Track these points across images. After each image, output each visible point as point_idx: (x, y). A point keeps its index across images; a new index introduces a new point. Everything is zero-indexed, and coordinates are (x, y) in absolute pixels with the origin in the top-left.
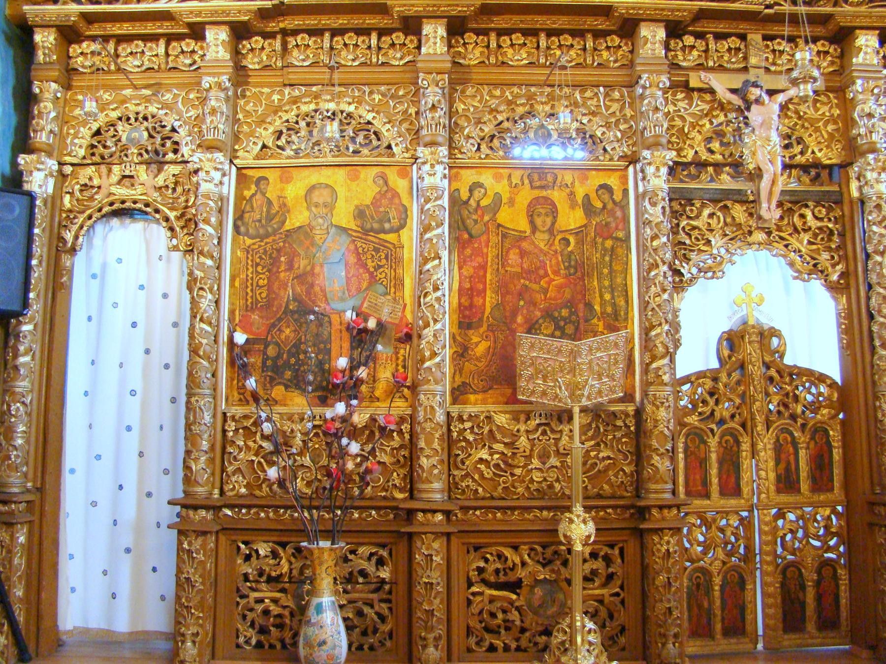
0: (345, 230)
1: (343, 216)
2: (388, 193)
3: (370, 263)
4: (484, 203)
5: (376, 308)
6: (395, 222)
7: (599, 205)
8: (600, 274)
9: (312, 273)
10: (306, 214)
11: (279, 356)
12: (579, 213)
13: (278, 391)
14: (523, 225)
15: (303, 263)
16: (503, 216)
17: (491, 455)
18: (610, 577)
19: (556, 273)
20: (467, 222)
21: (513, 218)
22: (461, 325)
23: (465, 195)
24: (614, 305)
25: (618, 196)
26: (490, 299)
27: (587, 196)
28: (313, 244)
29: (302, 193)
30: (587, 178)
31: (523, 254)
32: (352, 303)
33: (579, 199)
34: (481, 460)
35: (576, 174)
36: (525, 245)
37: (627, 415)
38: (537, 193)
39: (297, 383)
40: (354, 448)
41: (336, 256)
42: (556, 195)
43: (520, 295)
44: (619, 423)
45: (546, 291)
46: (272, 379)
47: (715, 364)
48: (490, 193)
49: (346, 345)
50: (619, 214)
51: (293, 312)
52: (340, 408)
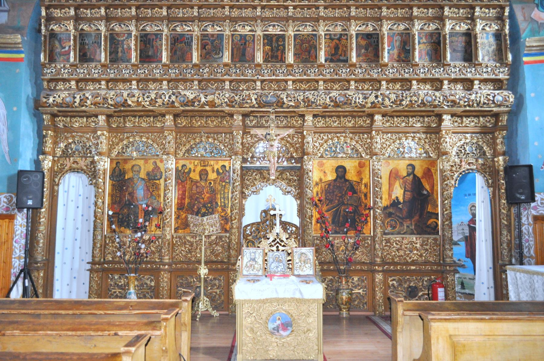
0: (143, 179)
1: (143, 175)
2: (157, 168)
3: (151, 190)
4: (186, 171)
5: (152, 203)
6: (159, 177)
7: (221, 171)
8: (221, 193)
9: (133, 192)
10: (131, 174)
11: (123, 218)
12: (215, 174)
13: (122, 229)
14: (198, 178)
15: (130, 189)
16: (192, 175)
17: (185, 248)
18: (220, 285)
19: (207, 193)
20: (182, 176)
21: (195, 176)
22: (178, 209)
23: (180, 168)
24: (224, 203)
25: (227, 169)
26: (187, 201)
27: (218, 169)
28: (134, 183)
29: (130, 167)
30: (218, 163)
31: (197, 187)
32: (145, 202)
33: (215, 170)
34: (182, 250)
35: (215, 162)
36: (198, 184)
37: (226, 237)
38: (202, 168)
39: (128, 226)
40: (143, 246)
41: (140, 187)
42: (209, 169)
43: (196, 200)
44: (223, 239)
45: (203, 199)
46: (121, 225)
47: (260, 221)
48: (188, 168)
49: (143, 215)
50: (227, 174)
51: (127, 205)
52: (139, 234)
